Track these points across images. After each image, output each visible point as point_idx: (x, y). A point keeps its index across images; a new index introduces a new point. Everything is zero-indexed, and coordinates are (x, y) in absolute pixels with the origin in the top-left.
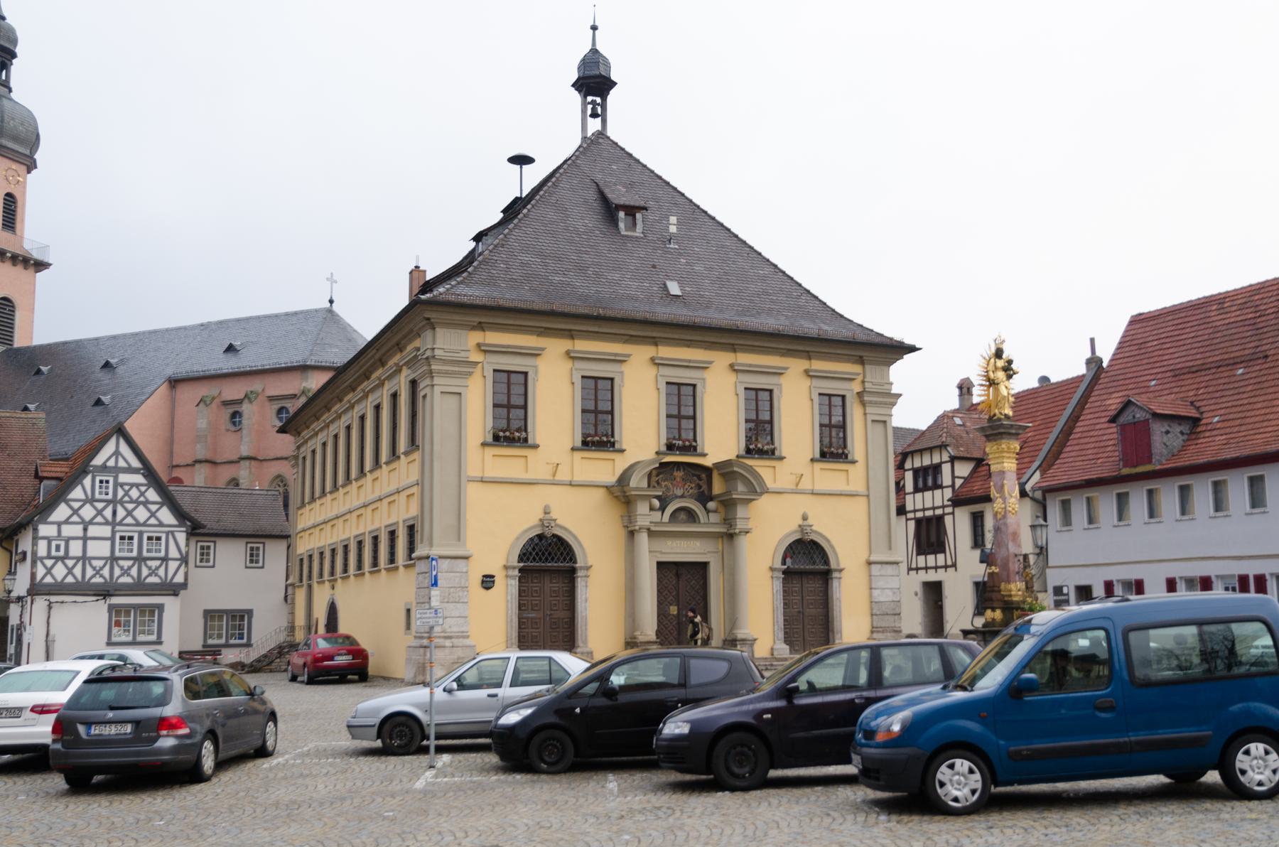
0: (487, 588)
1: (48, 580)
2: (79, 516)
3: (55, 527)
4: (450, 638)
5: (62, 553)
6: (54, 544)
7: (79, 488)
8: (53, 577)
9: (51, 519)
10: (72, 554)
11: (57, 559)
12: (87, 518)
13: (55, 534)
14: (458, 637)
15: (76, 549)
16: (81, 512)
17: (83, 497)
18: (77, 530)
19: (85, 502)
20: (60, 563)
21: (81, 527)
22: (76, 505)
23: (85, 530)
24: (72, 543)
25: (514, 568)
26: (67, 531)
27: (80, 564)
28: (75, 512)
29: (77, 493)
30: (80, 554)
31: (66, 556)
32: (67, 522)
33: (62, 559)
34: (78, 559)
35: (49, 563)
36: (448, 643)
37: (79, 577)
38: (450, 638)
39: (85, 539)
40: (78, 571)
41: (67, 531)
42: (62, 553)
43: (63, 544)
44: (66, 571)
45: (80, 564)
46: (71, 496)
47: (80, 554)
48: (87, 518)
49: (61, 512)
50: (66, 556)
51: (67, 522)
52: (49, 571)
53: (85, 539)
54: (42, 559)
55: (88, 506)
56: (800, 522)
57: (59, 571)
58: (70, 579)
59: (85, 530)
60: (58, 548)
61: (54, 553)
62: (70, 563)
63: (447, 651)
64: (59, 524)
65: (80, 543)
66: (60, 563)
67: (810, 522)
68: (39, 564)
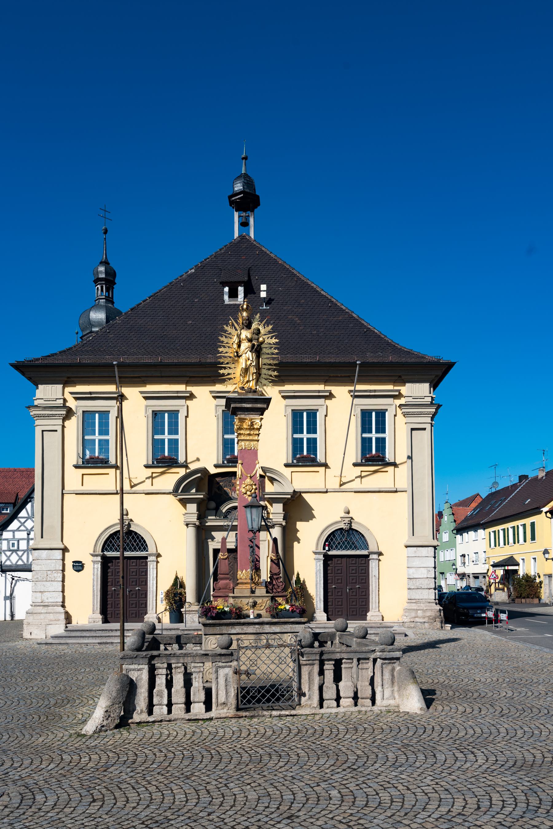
0: (78, 571)
1: (8, 563)
2: (25, 527)
3: (11, 533)
4: (48, 606)
5: (16, 548)
6: (11, 542)
7: (24, 510)
8: (10, 561)
9: (9, 528)
10: (21, 548)
11: (13, 551)
12: (29, 528)
13: (12, 537)
14: (53, 606)
15: (23, 545)
16: (25, 524)
17: (27, 516)
18: (24, 535)
19: (27, 518)
20: (14, 554)
21: (26, 533)
22: (23, 520)
23: (28, 534)
24: (20, 542)
25: (97, 556)
26: (18, 535)
27: (26, 554)
28: (23, 524)
29: (23, 513)
30: (25, 548)
31: (18, 550)
32: (18, 530)
33: (15, 551)
34: (24, 551)
35: (8, 553)
36: (44, 610)
37: (25, 561)
38: (48, 606)
39: (28, 540)
40: (24, 558)
41: (18, 535)
42: (16, 548)
43: (16, 543)
44: (11, 558)
45: (26, 554)
46: (20, 515)
47: (25, 548)
48: (29, 528)
49: (15, 525)
50: (18, 550)
51: (18, 530)
52: (8, 558)
53: (28, 540)
54: (4, 551)
55: (29, 521)
56: (343, 515)
57: (14, 558)
58: (20, 563)
59: (28, 534)
60: (13, 545)
61: (11, 548)
62: (20, 553)
63: (42, 616)
64: (14, 531)
65: (26, 541)
66: (14, 554)
67: (350, 515)
68: (3, 554)
